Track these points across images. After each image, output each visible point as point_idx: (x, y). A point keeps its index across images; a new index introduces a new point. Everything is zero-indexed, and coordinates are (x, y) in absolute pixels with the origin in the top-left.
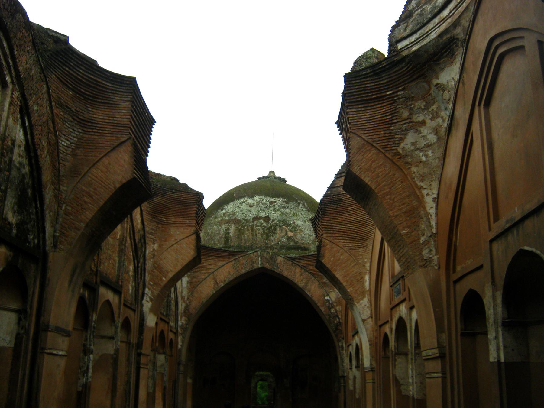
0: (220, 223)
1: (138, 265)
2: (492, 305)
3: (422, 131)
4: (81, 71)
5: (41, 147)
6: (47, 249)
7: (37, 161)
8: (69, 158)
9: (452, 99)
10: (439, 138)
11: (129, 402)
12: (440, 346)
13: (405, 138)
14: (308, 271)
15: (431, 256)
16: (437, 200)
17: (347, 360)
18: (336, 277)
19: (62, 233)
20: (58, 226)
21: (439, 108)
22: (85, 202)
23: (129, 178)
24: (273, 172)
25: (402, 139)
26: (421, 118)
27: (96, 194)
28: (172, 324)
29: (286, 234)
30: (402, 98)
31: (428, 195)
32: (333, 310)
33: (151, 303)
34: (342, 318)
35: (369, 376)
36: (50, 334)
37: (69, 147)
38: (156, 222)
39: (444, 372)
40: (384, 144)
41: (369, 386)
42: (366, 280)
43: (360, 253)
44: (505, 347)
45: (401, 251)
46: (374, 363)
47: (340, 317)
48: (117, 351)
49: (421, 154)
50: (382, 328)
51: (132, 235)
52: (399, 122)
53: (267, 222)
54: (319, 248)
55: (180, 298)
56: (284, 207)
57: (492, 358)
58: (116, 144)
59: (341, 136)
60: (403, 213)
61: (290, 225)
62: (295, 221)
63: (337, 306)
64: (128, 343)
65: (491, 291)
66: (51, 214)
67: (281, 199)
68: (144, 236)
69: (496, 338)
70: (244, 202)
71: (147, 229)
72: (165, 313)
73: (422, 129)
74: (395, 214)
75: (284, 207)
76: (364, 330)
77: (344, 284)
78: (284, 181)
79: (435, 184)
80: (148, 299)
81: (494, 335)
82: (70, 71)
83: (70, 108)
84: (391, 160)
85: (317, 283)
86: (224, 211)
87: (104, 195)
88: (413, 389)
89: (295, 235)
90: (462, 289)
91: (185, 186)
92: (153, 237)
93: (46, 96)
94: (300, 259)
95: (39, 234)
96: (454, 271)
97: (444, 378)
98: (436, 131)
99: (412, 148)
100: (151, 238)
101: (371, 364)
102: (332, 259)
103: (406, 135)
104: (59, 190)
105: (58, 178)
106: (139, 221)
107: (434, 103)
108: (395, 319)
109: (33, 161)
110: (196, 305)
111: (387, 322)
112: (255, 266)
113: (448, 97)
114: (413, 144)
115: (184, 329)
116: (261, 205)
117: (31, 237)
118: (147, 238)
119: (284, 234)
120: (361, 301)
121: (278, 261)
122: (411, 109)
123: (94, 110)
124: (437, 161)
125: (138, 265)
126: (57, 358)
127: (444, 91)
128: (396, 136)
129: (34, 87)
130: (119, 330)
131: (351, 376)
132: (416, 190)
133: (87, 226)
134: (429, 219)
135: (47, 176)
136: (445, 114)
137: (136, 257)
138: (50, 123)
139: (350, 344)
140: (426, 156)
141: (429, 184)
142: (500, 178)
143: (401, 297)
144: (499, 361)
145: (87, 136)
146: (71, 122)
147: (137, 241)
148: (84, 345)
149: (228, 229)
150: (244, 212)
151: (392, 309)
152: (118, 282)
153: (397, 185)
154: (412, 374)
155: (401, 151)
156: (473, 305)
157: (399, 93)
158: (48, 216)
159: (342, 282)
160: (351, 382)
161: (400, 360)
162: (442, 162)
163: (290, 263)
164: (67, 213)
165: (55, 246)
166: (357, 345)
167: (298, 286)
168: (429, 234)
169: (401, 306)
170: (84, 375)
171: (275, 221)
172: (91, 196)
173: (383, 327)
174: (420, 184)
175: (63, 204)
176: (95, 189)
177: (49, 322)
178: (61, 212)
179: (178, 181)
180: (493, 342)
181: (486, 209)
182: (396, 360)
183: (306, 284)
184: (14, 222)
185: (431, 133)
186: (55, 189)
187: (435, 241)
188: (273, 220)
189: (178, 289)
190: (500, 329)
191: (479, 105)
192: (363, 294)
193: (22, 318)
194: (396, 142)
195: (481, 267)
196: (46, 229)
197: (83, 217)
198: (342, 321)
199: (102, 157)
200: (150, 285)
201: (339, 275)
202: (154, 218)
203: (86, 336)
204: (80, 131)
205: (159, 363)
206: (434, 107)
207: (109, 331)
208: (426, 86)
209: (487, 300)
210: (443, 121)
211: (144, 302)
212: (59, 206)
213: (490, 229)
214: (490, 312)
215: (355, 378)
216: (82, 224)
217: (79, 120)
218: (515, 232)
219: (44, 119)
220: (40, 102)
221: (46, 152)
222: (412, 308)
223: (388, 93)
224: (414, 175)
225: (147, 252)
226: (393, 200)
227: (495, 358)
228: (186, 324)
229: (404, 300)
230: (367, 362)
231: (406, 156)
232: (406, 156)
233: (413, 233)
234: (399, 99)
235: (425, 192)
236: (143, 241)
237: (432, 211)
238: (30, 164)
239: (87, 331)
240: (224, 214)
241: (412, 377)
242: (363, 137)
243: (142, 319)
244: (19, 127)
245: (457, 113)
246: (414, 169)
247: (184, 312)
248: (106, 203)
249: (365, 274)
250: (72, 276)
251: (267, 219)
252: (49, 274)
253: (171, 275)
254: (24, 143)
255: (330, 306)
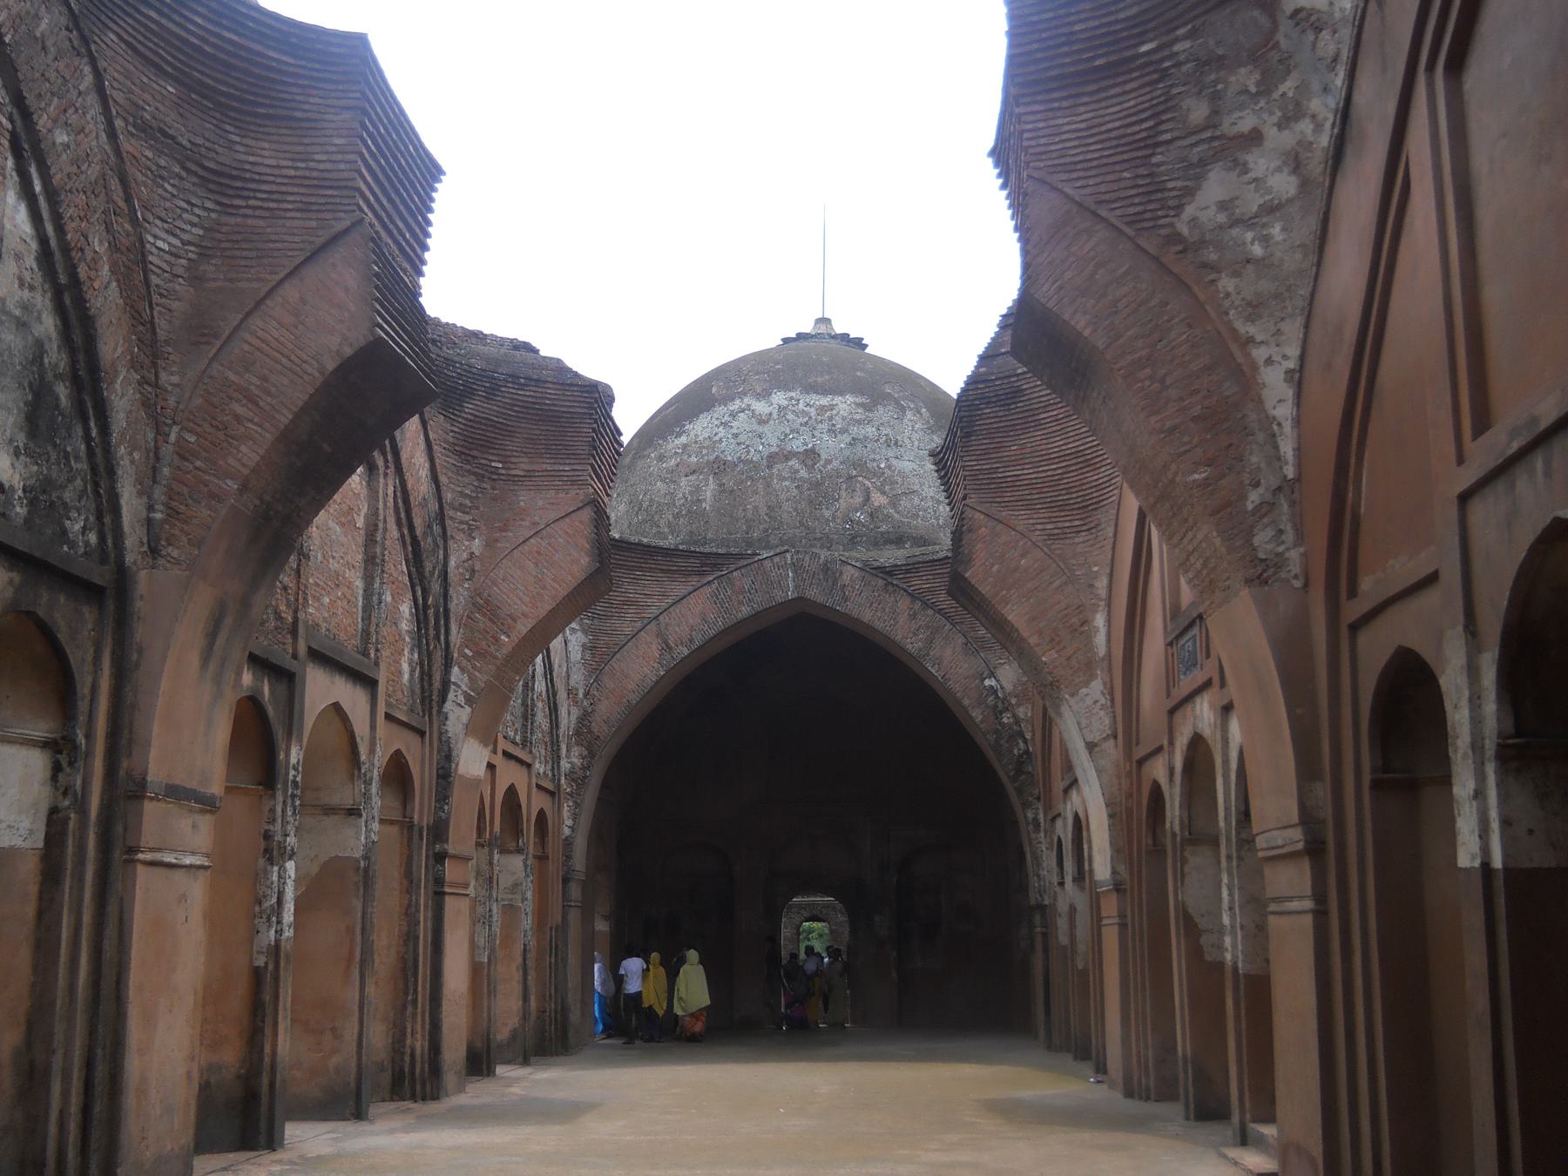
0: (671, 477)
1: (425, 599)
2: (1467, 693)
3: (1251, 165)
4: (199, 21)
5: (89, 255)
6: (129, 559)
7: (80, 302)
8: (180, 286)
9: (1345, 54)
10: (1305, 185)
11: (415, 991)
12: (1308, 818)
13: (1199, 188)
14: (932, 606)
15: (1280, 549)
16: (1297, 378)
17: (1049, 860)
18: (1006, 621)
19: (172, 513)
20: (159, 493)
21: (1303, 88)
22: (237, 418)
23: (362, 342)
24: (824, 321)
25: (1189, 193)
26: (1246, 123)
27: (269, 393)
28: (539, 767)
29: (867, 498)
30: (1187, 61)
31: (1269, 361)
33: (468, 709)
34: (1033, 739)
35: (1110, 907)
36: (149, 807)
37: (176, 256)
38: (475, 474)
39: (1320, 897)
40: (1132, 210)
41: (1111, 937)
43: (1079, 549)
44: (1506, 823)
45: (1190, 534)
46: (1122, 868)
47: (1028, 736)
48: (370, 848)
49: (1249, 235)
50: (1146, 768)
51: (403, 515)
52: (1178, 138)
53: (811, 468)
54: (957, 536)
55: (562, 695)
56: (859, 422)
57: (1467, 856)
58: (319, 241)
59: (1005, 193)
60: (1195, 419)
61: (878, 473)
62: (894, 462)
63: (1019, 705)
64: (408, 826)
65: (1463, 651)
66: (136, 455)
67: (850, 398)
68: (441, 516)
69: (1479, 794)
70: (743, 411)
71: (448, 496)
72: (518, 738)
73: (1250, 158)
74: (1168, 424)
75: (859, 422)
76: (1092, 774)
77: (1033, 640)
78: (859, 344)
79: (1293, 329)
80: (461, 700)
81: (1471, 785)
82: (164, 21)
83: (173, 138)
84: (1156, 259)
85: (960, 640)
86: (683, 439)
87: (291, 397)
88: (1234, 946)
89: (894, 503)
90: (1376, 648)
91: (559, 367)
92: (467, 518)
93: (92, 99)
94: (908, 571)
95: (99, 518)
96: (1353, 593)
97: (1320, 914)
98: (1295, 161)
99: (1221, 218)
100: (462, 522)
101: (1114, 872)
103: (1200, 178)
104: (157, 386)
105: (150, 351)
106: (424, 472)
107: (1288, 72)
108: (1182, 741)
109: (67, 301)
110: (610, 713)
111: (1160, 749)
112: (779, 596)
113: (1331, 48)
114: (1223, 206)
115: (578, 780)
116: (790, 416)
117: (78, 527)
118: (448, 522)
119: (858, 499)
120: (1084, 691)
121: (846, 578)
122: (1215, 97)
123: (246, 141)
124: (1298, 256)
125: (425, 599)
126: (178, 875)
127: (1318, 30)
128: (1170, 185)
129: (52, 75)
130: (374, 789)
131: (1062, 906)
132: (1234, 348)
133: (244, 488)
134: (1274, 435)
135: (113, 345)
136: (1323, 107)
137: (418, 577)
138: (114, 184)
139: (1059, 815)
140: (1266, 240)
141: (1273, 329)
142: (1493, 294)
143: (1198, 676)
144: (1486, 866)
145: (232, 220)
146: (181, 178)
147: (419, 532)
148: (267, 836)
149: (697, 489)
150: (742, 438)
151: (1172, 712)
152: (365, 654)
153: (1173, 334)
154: (1232, 901)
155: (1185, 231)
156: (1408, 693)
157: (1177, 48)
158: (126, 462)
159: (1025, 634)
160: (1062, 924)
161: (1198, 859)
162: (1313, 258)
163: (881, 582)
164: (183, 453)
165: (154, 551)
166: (1077, 818)
167: (903, 649)
168: (1274, 482)
169: (1198, 700)
170: (269, 919)
171: (835, 463)
172: (252, 400)
173: (1148, 764)
174: (1244, 328)
175: (170, 426)
176: (264, 379)
177: (145, 773)
178: (167, 450)
179: (536, 351)
180: (1467, 809)
181: (1448, 399)
182: (1184, 861)
183: (929, 642)
184: (18, 483)
185: (1279, 169)
186: (143, 381)
187: (1293, 504)
188: (828, 462)
189: (556, 667)
190: (1490, 769)
191: (1431, 67)
192: (1088, 669)
193: (64, 764)
194: (1171, 203)
195: (1432, 579)
196: (123, 502)
197: (231, 461)
198: (1035, 748)
199: (281, 282)
200: (465, 656)
201: (1015, 614)
202: (468, 463)
203: (272, 810)
204: (209, 205)
205: (505, 881)
206: (1288, 86)
207: (344, 796)
208: (1263, 20)
209: (1452, 680)
210: (1318, 127)
211: (448, 706)
212: (158, 432)
213: (1461, 460)
214: (1459, 717)
215: (1073, 909)
216: (229, 482)
217: (201, 172)
218: (1539, 465)
219: (93, 172)
220: (73, 118)
221: (105, 270)
222: (1227, 709)
223: (1144, 48)
224: (1227, 303)
225: (452, 563)
226: (1162, 381)
227: (1473, 858)
228: (583, 768)
229: (1207, 684)
230: (1102, 867)
231: (1203, 243)
232: (1203, 243)
233: (1223, 482)
234: (1177, 65)
235: (1260, 354)
236: (436, 529)
237: (1284, 412)
238: (60, 309)
239: (273, 796)
240: (685, 446)
241: (1231, 909)
242: (1067, 190)
243: (447, 758)
244: (11, 197)
245: (1359, 99)
246: (1227, 283)
247: (578, 733)
248: (297, 416)
250: (212, 636)
251: (810, 456)
252: (140, 632)
253: (523, 627)
254: (34, 246)
255: (1000, 705)
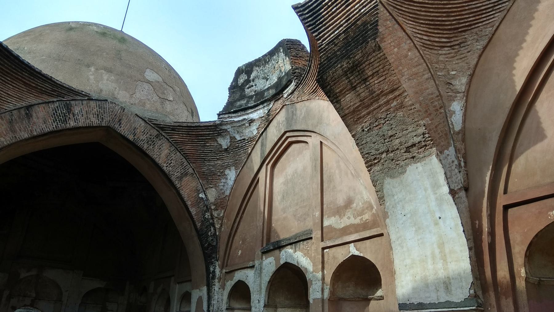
32: (207, 215)
34: (220, 228)
42: (454, 112)
43: (441, 58)
47: (217, 226)
63: (216, 209)
94: (173, 130)
102: (396, 50)
249: (452, 99)
